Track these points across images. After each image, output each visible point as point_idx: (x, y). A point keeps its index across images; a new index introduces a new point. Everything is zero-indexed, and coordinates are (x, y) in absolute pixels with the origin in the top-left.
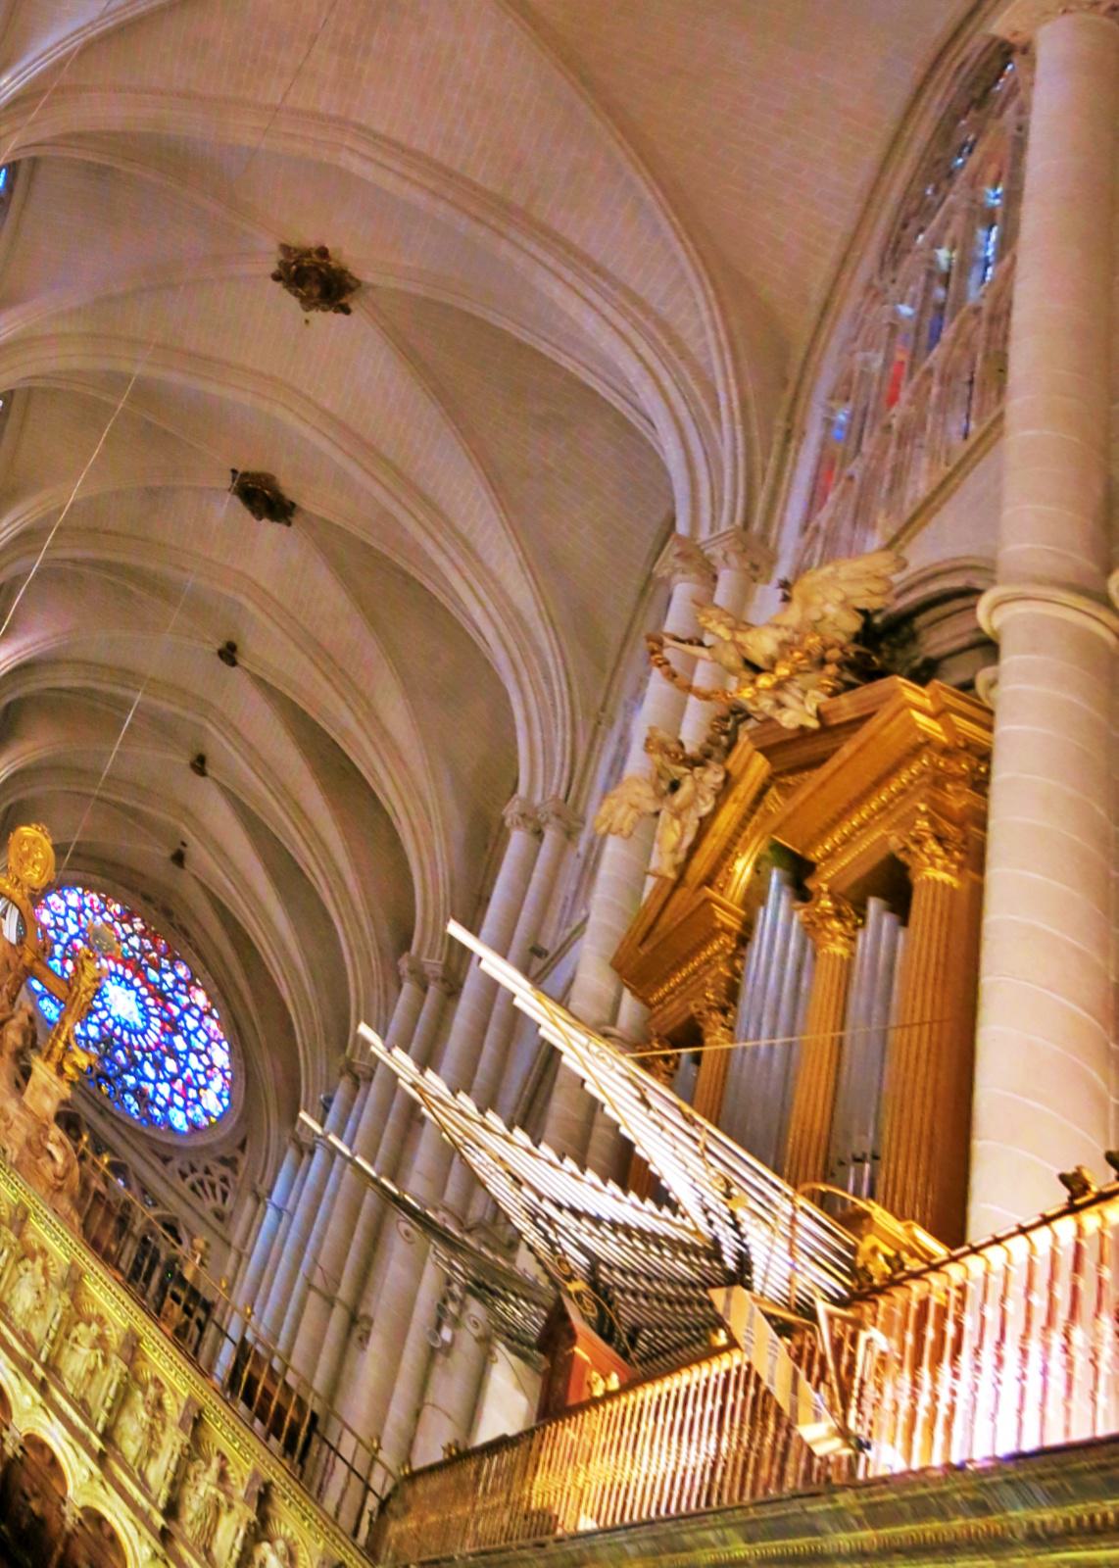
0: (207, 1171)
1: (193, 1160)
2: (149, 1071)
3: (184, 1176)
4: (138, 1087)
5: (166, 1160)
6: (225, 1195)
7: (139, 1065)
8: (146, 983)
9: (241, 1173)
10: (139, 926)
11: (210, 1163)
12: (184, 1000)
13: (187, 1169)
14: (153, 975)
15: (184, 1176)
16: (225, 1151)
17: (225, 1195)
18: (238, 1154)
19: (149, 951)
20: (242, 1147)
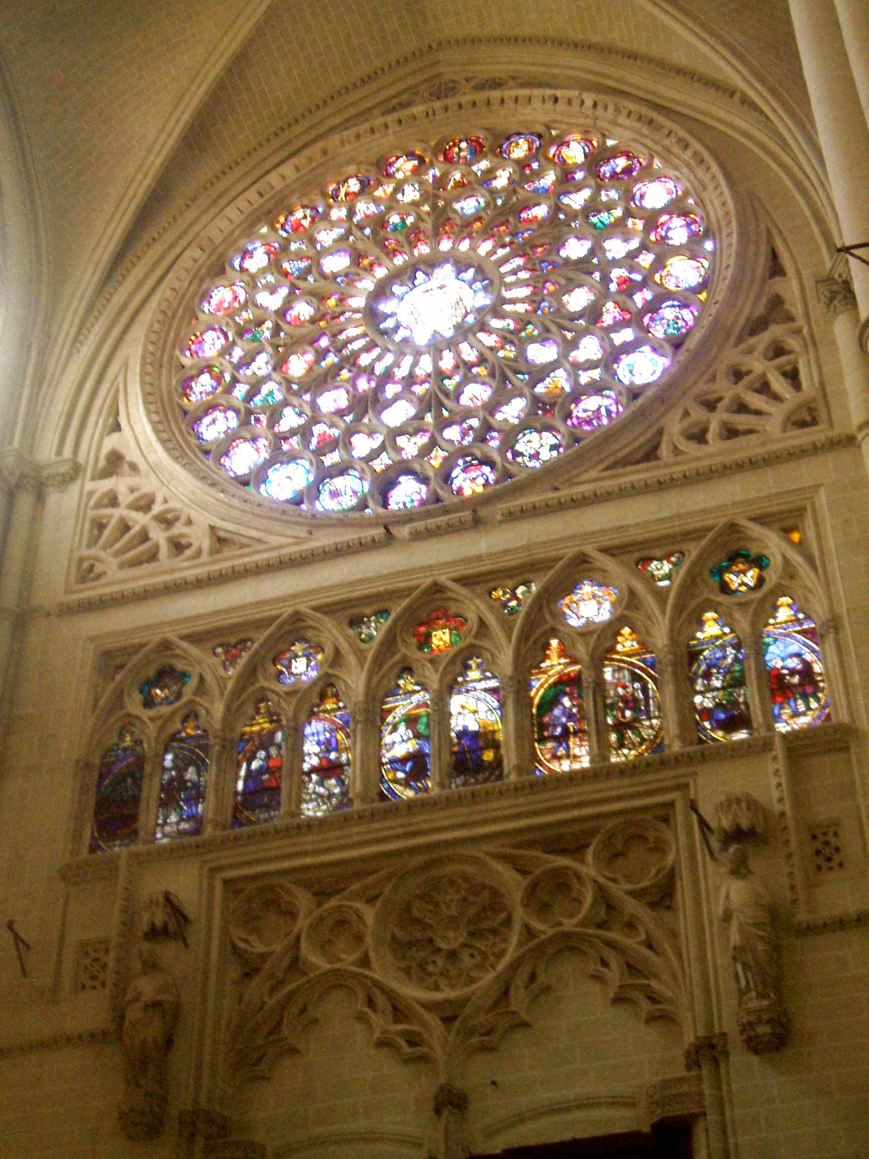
0: (738, 375)
1: (701, 387)
2: (541, 353)
3: (700, 437)
4: (537, 402)
5: (651, 454)
6: (792, 376)
7: (520, 364)
8: (465, 227)
9: (797, 310)
10: (404, 166)
11: (732, 356)
12: (549, 179)
13: (698, 414)
14: (468, 206)
15: (700, 437)
16: (750, 307)
17: (792, 376)
18: (777, 285)
19: (445, 177)
20: (776, 269)
